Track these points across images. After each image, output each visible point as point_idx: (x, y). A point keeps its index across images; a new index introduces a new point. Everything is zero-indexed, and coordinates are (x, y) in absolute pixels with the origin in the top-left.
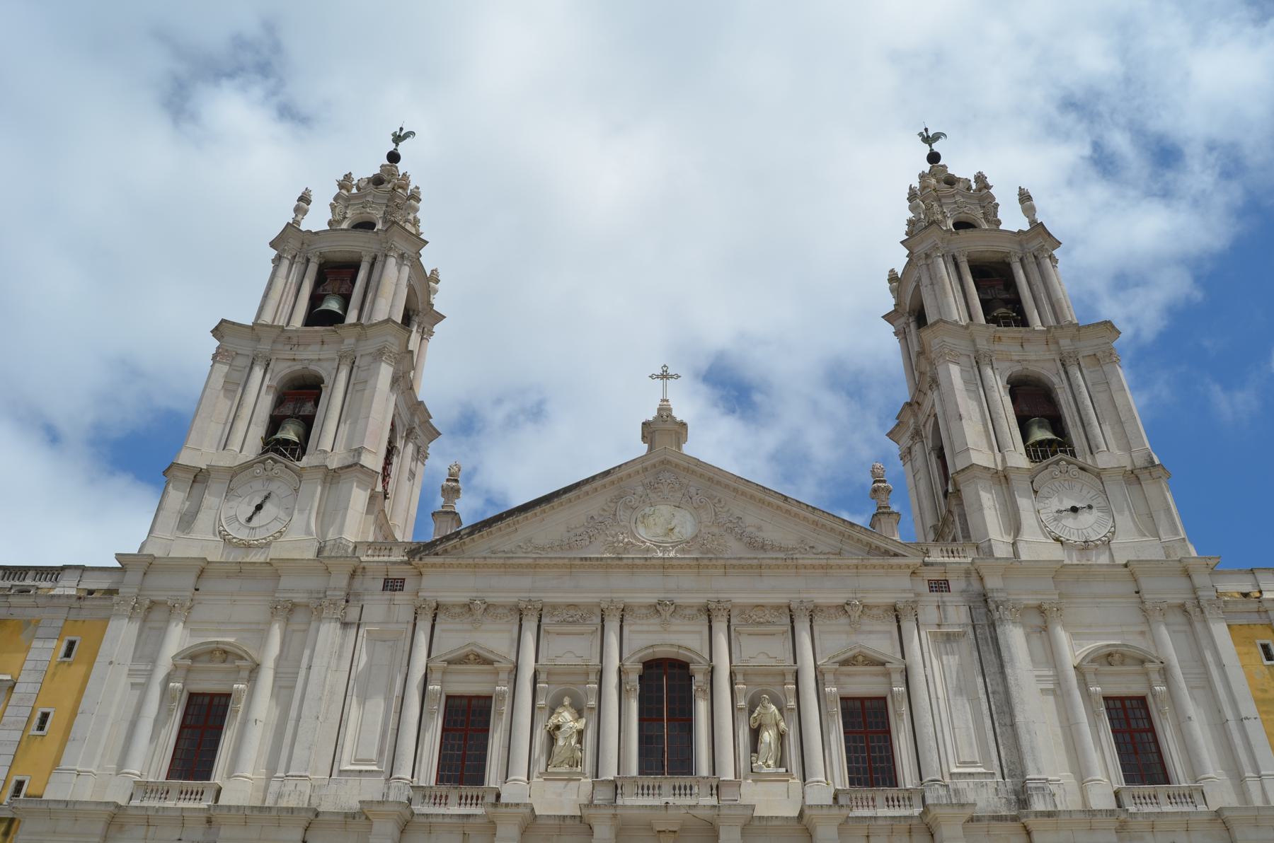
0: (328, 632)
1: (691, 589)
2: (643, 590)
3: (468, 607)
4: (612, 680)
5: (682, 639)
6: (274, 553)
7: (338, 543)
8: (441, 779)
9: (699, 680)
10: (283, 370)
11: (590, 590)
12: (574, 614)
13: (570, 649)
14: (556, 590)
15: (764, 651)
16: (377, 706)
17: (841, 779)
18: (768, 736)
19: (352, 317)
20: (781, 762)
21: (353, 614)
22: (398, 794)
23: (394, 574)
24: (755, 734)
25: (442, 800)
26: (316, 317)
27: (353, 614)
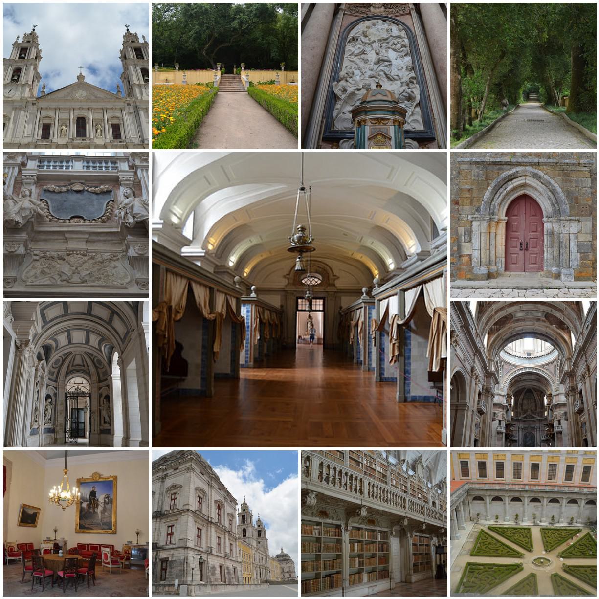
0: (22, 112)
1: (85, 105)
2: (77, 105)
3: (47, 108)
4: (72, 121)
5: (84, 114)
6: (13, 99)
7: (24, 97)
8: (42, 138)
9: (87, 121)
10: (14, 67)
11: (68, 105)
12: (65, 109)
13: (64, 115)
14: (62, 105)
15: (98, 116)
16: (31, 125)
17: (111, 138)
18: (99, 131)
19: (26, 58)
20: (101, 135)
21: (27, 109)
22: (35, 140)
23: (34, 102)
24: (97, 130)
25: (42, 142)
26: (20, 58)
27: (27, 109)
